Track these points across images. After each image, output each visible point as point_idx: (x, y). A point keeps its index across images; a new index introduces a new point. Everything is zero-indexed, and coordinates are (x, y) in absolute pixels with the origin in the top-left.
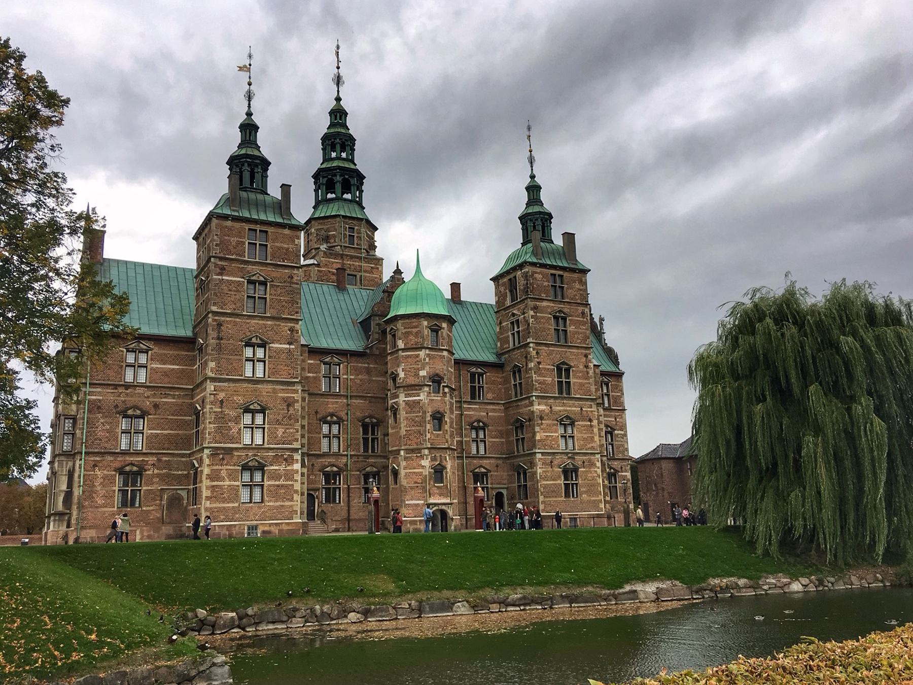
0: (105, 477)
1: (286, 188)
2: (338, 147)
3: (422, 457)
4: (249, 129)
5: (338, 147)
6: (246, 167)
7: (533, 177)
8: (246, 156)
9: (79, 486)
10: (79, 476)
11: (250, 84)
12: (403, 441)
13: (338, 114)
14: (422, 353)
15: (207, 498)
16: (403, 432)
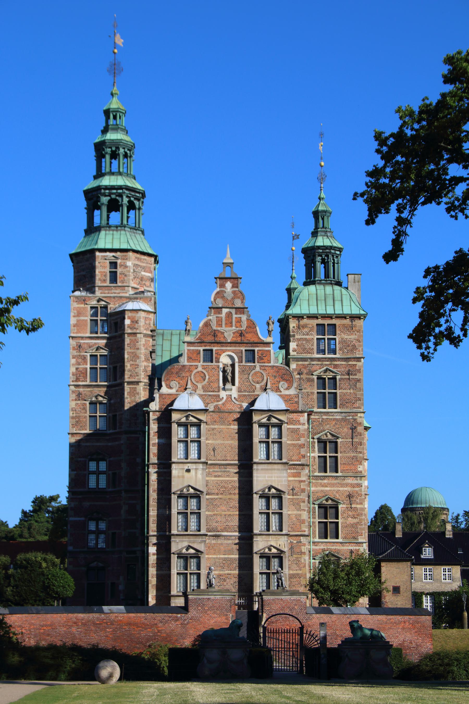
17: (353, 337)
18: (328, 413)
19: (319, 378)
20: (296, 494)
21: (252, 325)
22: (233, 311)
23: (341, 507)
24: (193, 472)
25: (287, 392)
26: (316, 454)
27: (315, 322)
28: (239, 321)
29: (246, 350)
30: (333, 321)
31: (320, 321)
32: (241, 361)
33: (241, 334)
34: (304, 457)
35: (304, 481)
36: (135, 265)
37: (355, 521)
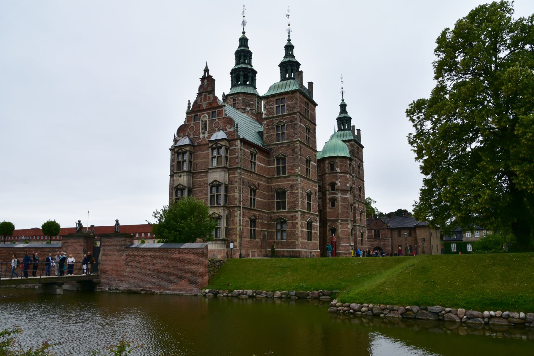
0: (246, 221)
1: (311, 84)
2: (242, 58)
3: (348, 224)
4: (289, 48)
5: (242, 58)
6: (289, 67)
7: (343, 100)
8: (289, 61)
9: (240, 225)
10: (240, 220)
11: (289, 25)
12: (340, 216)
13: (244, 41)
14: (348, 176)
15: (301, 237)
16: (340, 212)
17: (293, 102)
18: (281, 144)
19: (277, 127)
20: (233, 184)
21: (216, 98)
22: (207, 94)
23: (288, 192)
24: (182, 177)
25: (230, 130)
26: (276, 166)
27: (274, 99)
28: (209, 98)
29: (212, 112)
30: (284, 96)
31: (277, 98)
32: (209, 118)
33: (210, 104)
34: (237, 163)
35: (237, 177)
36: (243, 99)
37: (294, 199)
